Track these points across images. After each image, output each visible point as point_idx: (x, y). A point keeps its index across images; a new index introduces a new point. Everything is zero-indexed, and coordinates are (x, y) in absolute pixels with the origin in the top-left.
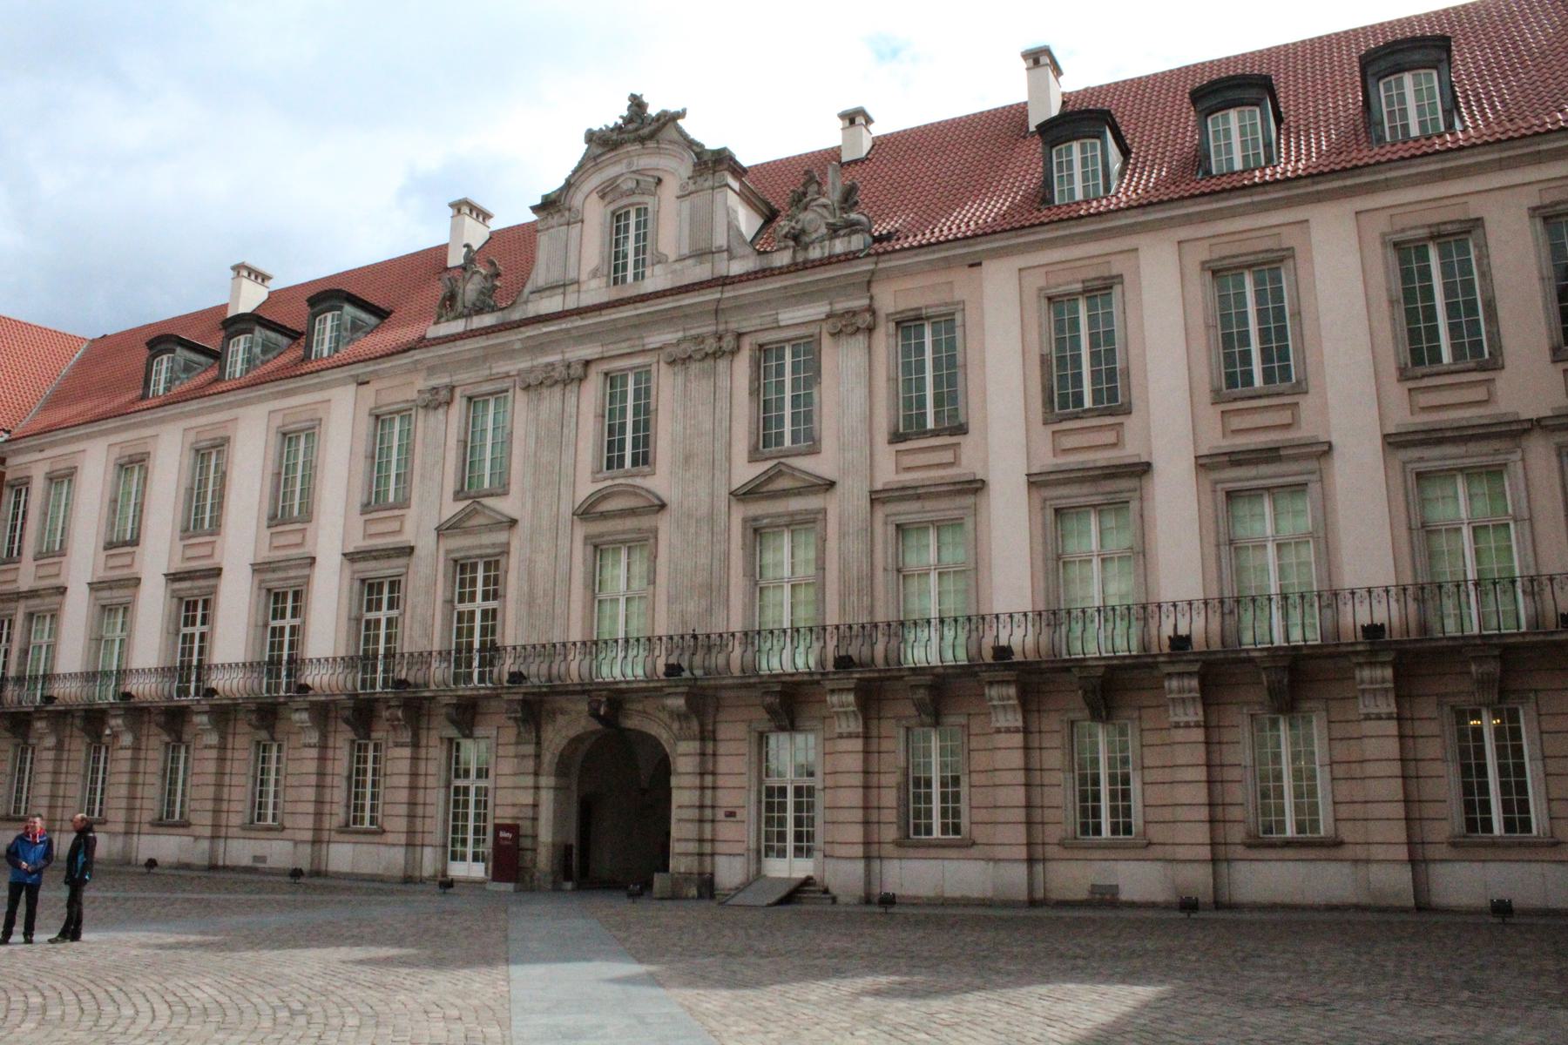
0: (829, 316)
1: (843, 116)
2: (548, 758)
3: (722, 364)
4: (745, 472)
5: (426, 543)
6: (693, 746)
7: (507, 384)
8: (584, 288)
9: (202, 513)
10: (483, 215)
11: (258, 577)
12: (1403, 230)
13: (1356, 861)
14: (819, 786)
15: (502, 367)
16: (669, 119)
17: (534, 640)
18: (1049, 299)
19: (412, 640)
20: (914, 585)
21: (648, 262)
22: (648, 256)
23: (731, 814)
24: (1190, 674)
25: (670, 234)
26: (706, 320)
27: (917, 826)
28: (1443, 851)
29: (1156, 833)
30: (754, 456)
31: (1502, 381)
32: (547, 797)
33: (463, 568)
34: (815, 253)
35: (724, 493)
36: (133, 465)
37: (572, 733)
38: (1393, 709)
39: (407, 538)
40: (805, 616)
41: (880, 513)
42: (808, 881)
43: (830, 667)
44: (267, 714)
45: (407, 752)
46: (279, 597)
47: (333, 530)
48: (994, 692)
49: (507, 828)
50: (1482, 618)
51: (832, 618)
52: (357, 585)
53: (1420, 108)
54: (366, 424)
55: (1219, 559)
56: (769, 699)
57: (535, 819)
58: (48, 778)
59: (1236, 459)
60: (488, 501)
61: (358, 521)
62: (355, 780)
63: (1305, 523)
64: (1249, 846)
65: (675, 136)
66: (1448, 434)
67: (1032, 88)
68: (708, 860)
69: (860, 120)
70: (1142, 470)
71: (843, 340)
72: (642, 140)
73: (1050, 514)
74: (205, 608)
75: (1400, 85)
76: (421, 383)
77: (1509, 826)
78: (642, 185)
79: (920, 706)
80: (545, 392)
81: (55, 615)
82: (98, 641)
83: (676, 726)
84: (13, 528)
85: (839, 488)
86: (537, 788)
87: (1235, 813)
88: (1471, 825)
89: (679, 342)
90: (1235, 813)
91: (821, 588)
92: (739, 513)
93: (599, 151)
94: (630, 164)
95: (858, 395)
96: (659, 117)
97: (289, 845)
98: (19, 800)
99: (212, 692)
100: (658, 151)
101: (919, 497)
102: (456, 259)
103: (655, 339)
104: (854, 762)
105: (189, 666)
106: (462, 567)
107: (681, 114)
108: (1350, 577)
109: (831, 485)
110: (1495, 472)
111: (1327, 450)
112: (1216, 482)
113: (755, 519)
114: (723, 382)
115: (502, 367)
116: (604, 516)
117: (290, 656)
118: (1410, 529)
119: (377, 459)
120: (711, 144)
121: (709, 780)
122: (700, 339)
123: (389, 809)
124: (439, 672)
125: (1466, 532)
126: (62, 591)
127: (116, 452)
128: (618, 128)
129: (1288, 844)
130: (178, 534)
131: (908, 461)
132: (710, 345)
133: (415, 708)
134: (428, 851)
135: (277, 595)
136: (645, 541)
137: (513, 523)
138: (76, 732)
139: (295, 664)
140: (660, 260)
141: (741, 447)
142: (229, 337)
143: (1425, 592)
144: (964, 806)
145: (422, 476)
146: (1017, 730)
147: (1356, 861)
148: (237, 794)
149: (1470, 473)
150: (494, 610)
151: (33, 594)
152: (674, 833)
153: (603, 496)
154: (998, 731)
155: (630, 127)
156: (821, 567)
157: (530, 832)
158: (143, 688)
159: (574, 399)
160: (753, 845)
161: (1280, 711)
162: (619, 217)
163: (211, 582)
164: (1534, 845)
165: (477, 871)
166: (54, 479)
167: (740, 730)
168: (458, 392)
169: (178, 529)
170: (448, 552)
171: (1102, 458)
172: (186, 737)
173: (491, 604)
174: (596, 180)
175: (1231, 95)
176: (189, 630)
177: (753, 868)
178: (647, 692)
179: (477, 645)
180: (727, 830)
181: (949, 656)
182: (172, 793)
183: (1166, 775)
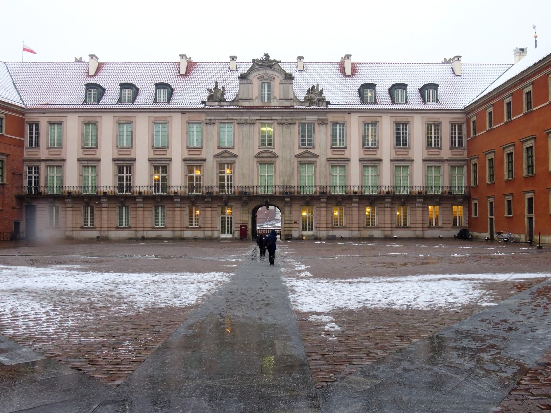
0: (318, 120)
3: (292, 126)
4: (298, 152)
5: (210, 159)
11: (150, 162)
29: (380, 226)
31: (442, 151)
39: (203, 156)
49: (244, 226)
59: (398, 160)
80: (245, 125)
103: (274, 118)
110: (439, 167)
116: (262, 157)
122: (287, 120)
125: (433, 177)
129: (402, 228)
132: (290, 122)
140: (275, 98)
149: (435, 167)
153: (262, 152)
155: (266, 62)
156: (315, 172)
158: (109, 190)
170: (217, 161)
175: (400, 87)
180: (294, 225)
181: (342, 192)
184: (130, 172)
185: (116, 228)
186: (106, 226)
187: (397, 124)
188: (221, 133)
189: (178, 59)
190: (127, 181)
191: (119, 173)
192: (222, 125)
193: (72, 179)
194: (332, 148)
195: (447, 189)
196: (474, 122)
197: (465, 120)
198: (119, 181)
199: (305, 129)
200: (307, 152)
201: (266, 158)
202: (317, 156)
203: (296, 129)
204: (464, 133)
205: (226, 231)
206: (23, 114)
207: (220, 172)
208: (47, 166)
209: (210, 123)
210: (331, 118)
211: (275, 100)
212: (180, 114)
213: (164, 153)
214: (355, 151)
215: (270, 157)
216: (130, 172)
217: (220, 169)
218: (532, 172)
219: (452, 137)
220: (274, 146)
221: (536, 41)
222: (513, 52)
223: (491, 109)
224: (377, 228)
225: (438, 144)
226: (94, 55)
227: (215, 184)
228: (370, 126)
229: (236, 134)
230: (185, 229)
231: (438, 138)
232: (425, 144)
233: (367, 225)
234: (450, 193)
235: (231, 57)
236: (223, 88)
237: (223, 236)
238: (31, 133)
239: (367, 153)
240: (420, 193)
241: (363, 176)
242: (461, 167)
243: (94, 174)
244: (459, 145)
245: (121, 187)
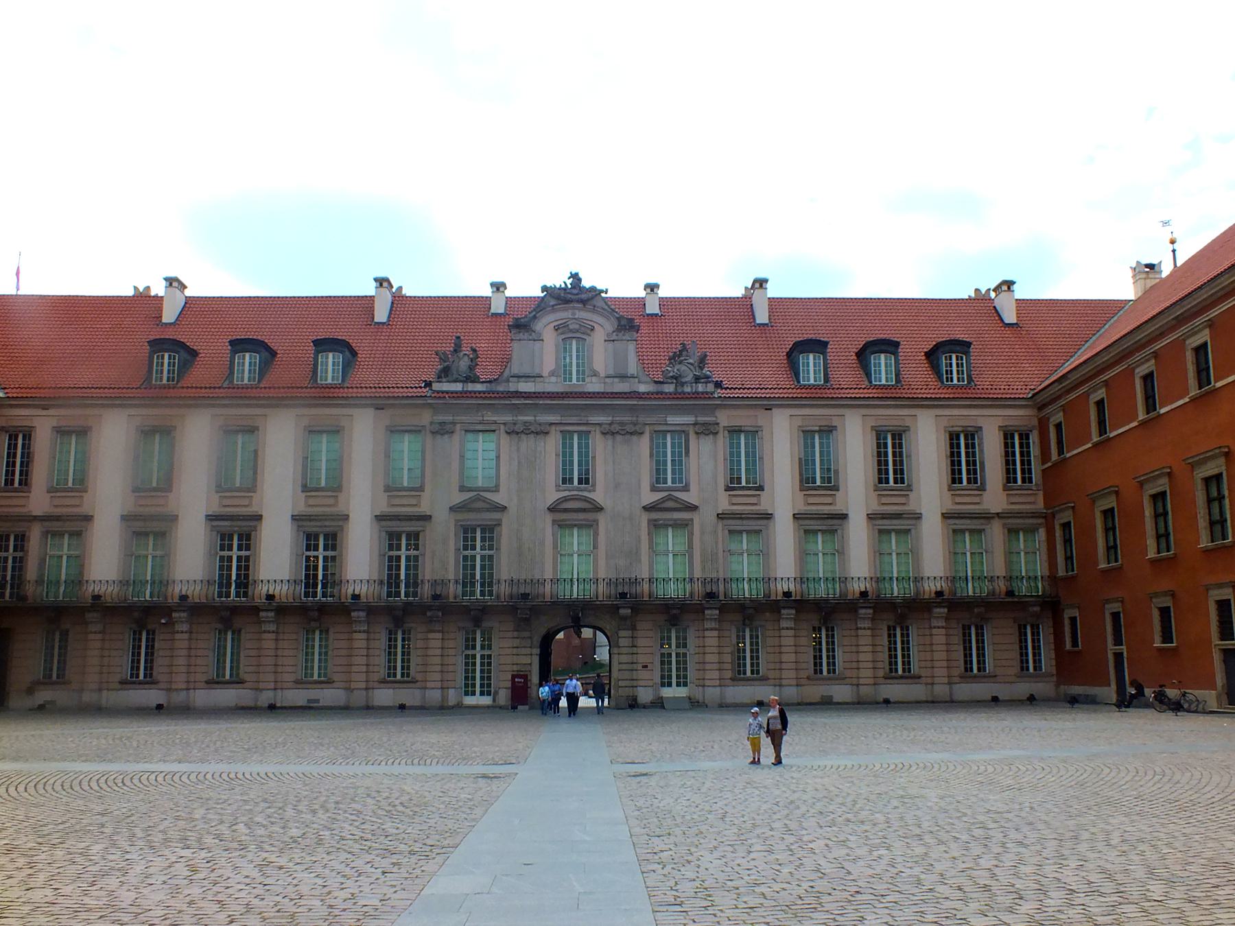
0: (695, 424)
3: (635, 438)
4: (650, 498)
13: (927, 684)
17: (524, 577)
26: (621, 411)
29: (848, 673)
30: (654, 489)
33: (466, 531)
34: (688, 389)
39: (424, 509)
51: (698, 574)
52: (384, 534)
59: (884, 516)
70: (844, 517)
71: (702, 436)
80: (523, 436)
81: (78, 534)
82: (131, 556)
88: (966, 670)
89: (610, 424)
106: (467, 533)
110: (980, 531)
116: (566, 510)
122: (622, 424)
125: (968, 554)
129: (901, 677)
132: (629, 428)
136: (591, 526)
140: (595, 374)
147: (927, 684)
153: (566, 499)
155: (575, 291)
156: (691, 546)
158: (196, 593)
170: (457, 521)
171: (826, 509)
180: (643, 674)
184: (248, 549)
185: (207, 682)
186: (183, 677)
187: (880, 434)
188: (468, 455)
189: (369, 289)
190: (239, 568)
191: (222, 549)
192: (470, 436)
193: (105, 564)
194: (728, 489)
195: (1002, 586)
196: (1058, 426)
197: (1035, 422)
198: (221, 568)
199: (665, 446)
200: (670, 498)
201: (575, 512)
202: (694, 508)
203: (643, 445)
204: (1035, 450)
205: (478, 692)
207: (465, 548)
208: (45, 534)
209: (443, 430)
210: (724, 418)
211: (594, 379)
212: (370, 412)
213: (331, 501)
214: (783, 495)
215: (584, 510)
216: (248, 548)
217: (465, 539)
218: (1224, 537)
220: (594, 485)
221: (1174, 251)
222: (1130, 274)
223: (1101, 394)
224: (841, 679)
225: (976, 479)
226: (177, 280)
227: (451, 576)
230: (376, 685)
231: (975, 464)
232: (946, 478)
233: (816, 672)
234: (1010, 593)
235: (492, 285)
236: (474, 351)
237: (469, 700)
239: (811, 500)
240: (939, 594)
241: (803, 556)
242: (1031, 530)
243: (158, 553)
244: (1024, 481)
245: (224, 582)
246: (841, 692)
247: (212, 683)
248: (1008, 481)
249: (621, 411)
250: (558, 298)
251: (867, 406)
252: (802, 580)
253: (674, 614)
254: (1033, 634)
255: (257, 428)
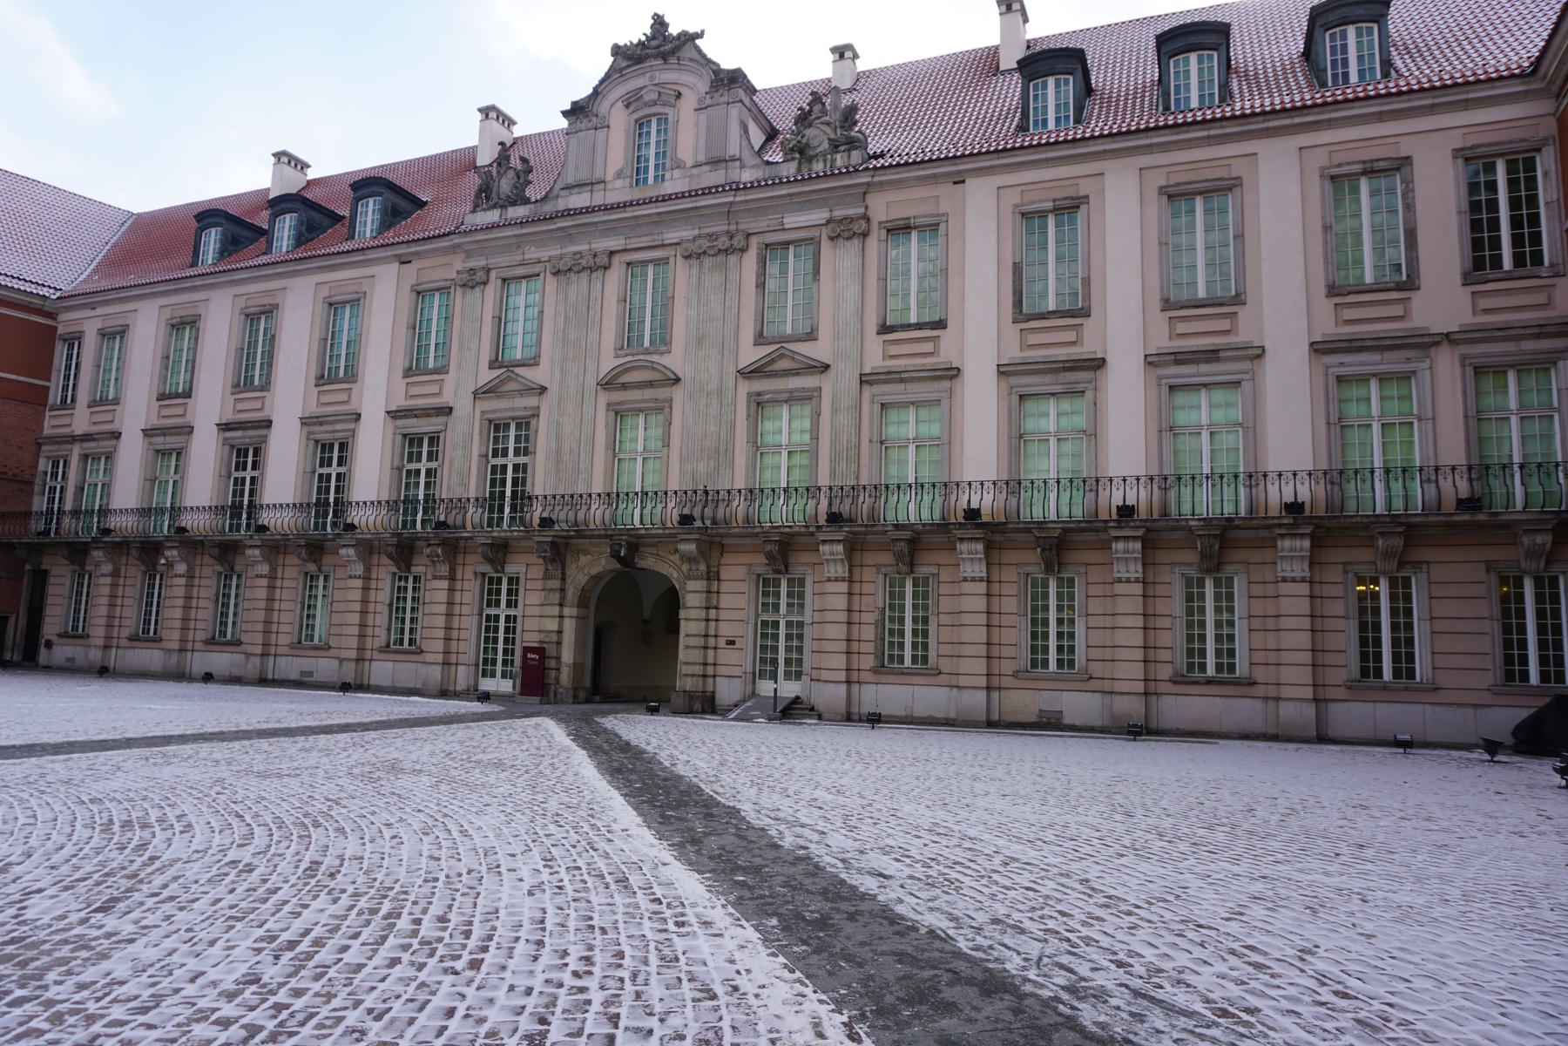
0: (829, 222)
1: (833, 50)
2: (572, 592)
3: (733, 259)
4: (750, 354)
5: (463, 405)
6: (700, 585)
7: (537, 268)
8: (609, 186)
9: (252, 374)
10: (508, 122)
11: (306, 429)
12: (1339, 165)
13: (1266, 699)
14: (808, 620)
15: (532, 253)
16: (689, 38)
18: (1023, 214)
19: (448, 488)
20: (894, 455)
21: (668, 166)
22: (668, 161)
23: (732, 643)
24: (1135, 538)
25: (688, 144)
27: (891, 657)
28: (1340, 693)
29: (1096, 669)
30: (760, 339)
31: (1417, 299)
32: (569, 626)
35: (732, 371)
36: (185, 325)
37: (594, 571)
38: (1307, 574)
39: (446, 398)
40: (799, 478)
41: (868, 392)
42: (797, 700)
43: (822, 521)
44: (315, 549)
45: (445, 584)
46: (326, 447)
47: (377, 390)
48: (963, 547)
50: (1389, 500)
51: (824, 480)
52: (399, 438)
53: (1360, 58)
54: (407, 299)
55: (1160, 439)
56: (769, 547)
57: (559, 643)
58: (105, 601)
59: (1180, 358)
60: (517, 370)
61: (401, 384)
62: (396, 608)
63: (1236, 414)
64: (1175, 683)
65: (695, 55)
66: (1369, 343)
67: (1004, 34)
68: (710, 680)
69: (848, 54)
70: (1098, 364)
72: (664, 57)
73: (1015, 398)
74: (255, 455)
75: (1344, 36)
76: (458, 263)
77: (1397, 673)
78: (663, 97)
79: (899, 558)
80: (573, 276)
81: (109, 457)
82: (152, 481)
83: (685, 567)
84: (67, 377)
85: (832, 370)
86: (561, 617)
87: (1165, 655)
88: (1365, 672)
89: (694, 239)
90: (1165, 655)
91: (814, 453)
92: (745, 387)
93: (624, 64)
94: (652, 78)
95: (852, 292)
96: (679, 35)
97: (336, 662)
98: (76, 619)
99: (263, 529)
100: (680, 67)
101: (902, 381)
102: (484, 159)
103: (672, 236)
104: (840, 602)
105: (241, 503)
107: (700, 35)
108: (1272, 464)
109: (827, 367)
110: (1406, 377)
111: (1259, 354)
112: (1161, 378)
113: (759, 394)
114: (733, 276)
115: (532, 253)
116: (624, 387)
117: (336, 499)
118: (1328, 423)
119: (417, 328)
120: (727, 64)
121: (713, 613)
123: (426, 633)
124: (474, 515)
125: (1376, 427)
126: (117, 435)
127: (167, 313)
128: (640, 43)
129: (1209, 682)
130: (229, 389)
131: (893, 350)
132: (723, 242)
133: (452, 546)
134: (461, 669)
135: (324, 446)
136: (663, 408)
137: (543, 389)
138: (132, 561)
139: (341, 506)
140: (679, 165)
141: (748, 334)
142: (275, 216)
143: (1335, 477)
144: (932, 640)
145: (461, 348)
146: (981, 580)
147: (1266, 699)
148: (285, 617)
149: (1383, 379)
150: (525, 465)
151: (87, 437)
152: (681, 656)
154: (965, 579)
155: (654, 43)
156: (815, 438)
157: (554, 653)
158: (196, 523)
159: (599, 286)
160: (749, 669)
161: (1208, 571)
162: (641, 124)
163: (263, 432)
164: (1420, 689)
165: (506, 686)
166: (107, 335)
167: (740, 572)
168: (493, 274)
169: (230, 383)
170: (483, 413)
172: (237, 568)
173: (521, 460)
174: (621, 90)
175: (1193, 39)
176: (240, 474)
177: (749, 688)
178: (664, 540)
179: (508, 493)
180: (727, 656)
182: (224, 615)
183: (1108, 621)
185: (130, 639)
194: (884, 329)
197: (1550, 127)
201: (638, 387)
205: (499, 668)
206: (52, 316)
210: (882, 207)
211: (676, 173)
212: (394, 267)
215: (650, 384)
219: (1475, 225)
228: (1051, 221)
229: (549, 312)
230: (376, 655)
234: (1469, 504)
236: (524, 160)
237: (487, 685)
238: (68, 367)
239: (1034, 339)
241: (1017, 440)
244: (1519, 260)
246: (1076, 704)
247: (211, 642)
248: (1478, 264)
249: (722, 224)
250: (629, 58)
251: (1150, 149)
252: (1013, 485)
253: (783, 551)
254: (1539, 598)
255: (276, 306)
